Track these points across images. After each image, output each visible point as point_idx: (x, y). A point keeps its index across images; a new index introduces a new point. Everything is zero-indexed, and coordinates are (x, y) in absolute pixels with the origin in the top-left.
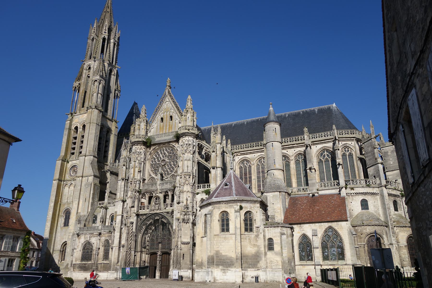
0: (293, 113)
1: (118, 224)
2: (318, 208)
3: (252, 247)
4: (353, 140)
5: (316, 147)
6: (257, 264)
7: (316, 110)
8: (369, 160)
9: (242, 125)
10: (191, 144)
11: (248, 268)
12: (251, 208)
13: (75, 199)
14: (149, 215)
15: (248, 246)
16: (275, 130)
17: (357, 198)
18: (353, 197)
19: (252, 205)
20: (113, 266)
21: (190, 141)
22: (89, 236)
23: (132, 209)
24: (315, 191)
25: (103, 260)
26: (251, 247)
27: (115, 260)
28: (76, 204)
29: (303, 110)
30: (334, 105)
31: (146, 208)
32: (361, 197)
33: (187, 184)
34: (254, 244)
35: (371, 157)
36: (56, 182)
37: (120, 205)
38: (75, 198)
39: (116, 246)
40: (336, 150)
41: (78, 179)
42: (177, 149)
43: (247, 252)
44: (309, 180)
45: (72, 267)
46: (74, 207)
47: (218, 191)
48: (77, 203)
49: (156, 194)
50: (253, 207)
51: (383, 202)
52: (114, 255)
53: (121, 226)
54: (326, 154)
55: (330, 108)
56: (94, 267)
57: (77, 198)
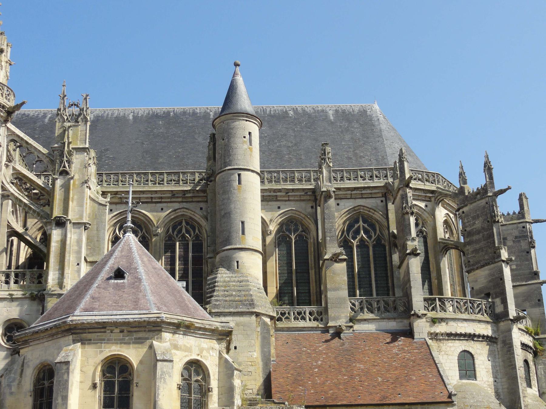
0: (268, 110)
2: (362, 366)
4: (430, 198)
5: (338, 204)
7: (331, 112)
8: (476, 251)
9: (120, 120)
12: (202, 350)
16: (247, 136)
17: (451, 347)
18: (441, 345)
24: (342, 322)
29: (293, 106)
30: (376, 107)
32: (459, 346)
35: (482, 244)
40: (407, 213)
44: (330, 290)
47: (91, 292)
50: (208, 350)
51: (510, 362)
54: (361, 227)
55: (365, 111)
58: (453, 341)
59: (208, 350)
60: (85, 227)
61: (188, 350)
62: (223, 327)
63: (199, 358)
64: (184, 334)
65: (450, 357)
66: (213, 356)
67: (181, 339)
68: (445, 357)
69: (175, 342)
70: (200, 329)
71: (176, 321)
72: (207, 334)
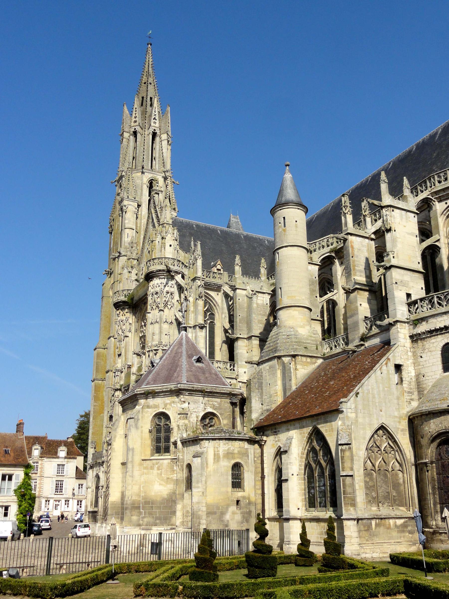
3: (164, 483)
6: (171, 517)
10: (159, 292)
11: (152, 525)
12: (166, 405)
15: (156, 482)
17: (433, 343)
18: (425, 343)
19: (168, 400)
21: (158, 286)
26: (160, 484)
34: (168, 478)
43: (153, 494)
50: (170, 404)
58: (436, 337)
59: (170, 404)
60: (199, 327)
61: (156, 406)
62: (175, 387)
63: (164, 411)
64: (153, 398)
65: (433, 353)
66: (174, 407)
67: (151, 401)
68: (429, 354)
69: (148, 404)
70: (162, 392)
71: (143, 392)
72: (168, 395)
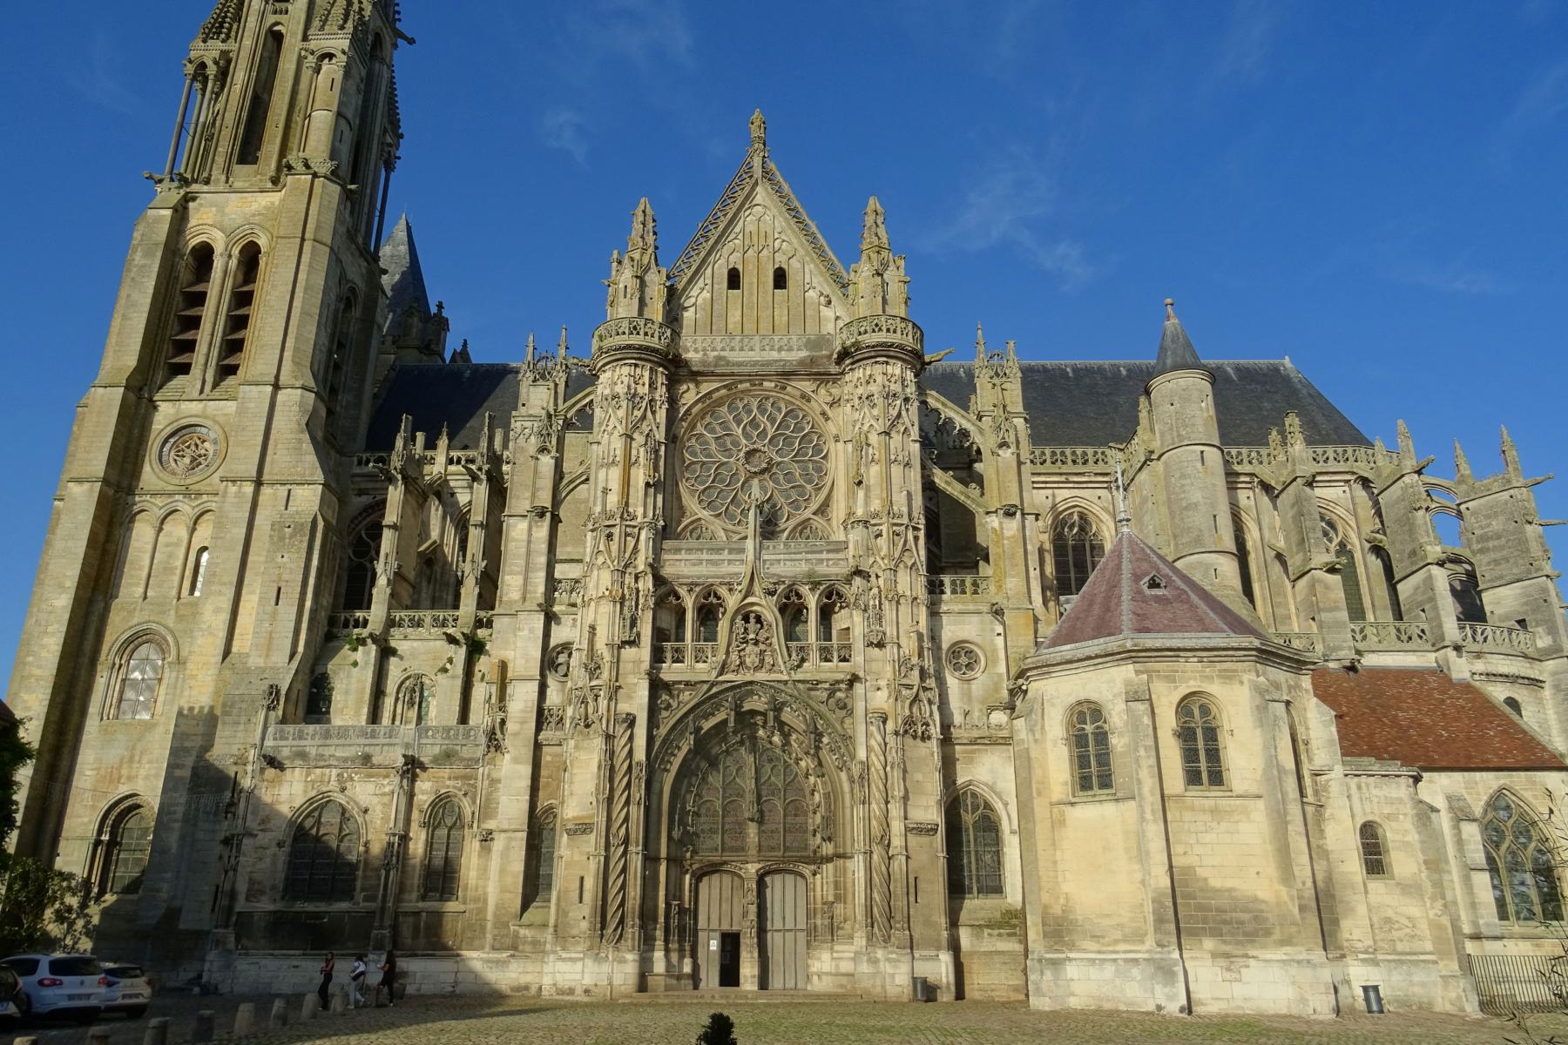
1: (523, 723)
13: (215, 588)
14: (714, 690)
20: (495, 926)
22: (334, 772)
23: (628, 652)
25: (423, 898)
27: (507, 895)
28: (217, 611)
31: (689, 655)
33: (909, 564)
36: (91, 490)
37: (531, 631)
38: (216, 580)
39: (513, 827)
41: (233, 489)
42: (824, 414)
45: (231, 930)
46: (204, 627)
48: (227, 605)
49: (745, 597)
52: (503, 871)
53: (539, 729)
56: (381, 927)
57: (225, 579)
